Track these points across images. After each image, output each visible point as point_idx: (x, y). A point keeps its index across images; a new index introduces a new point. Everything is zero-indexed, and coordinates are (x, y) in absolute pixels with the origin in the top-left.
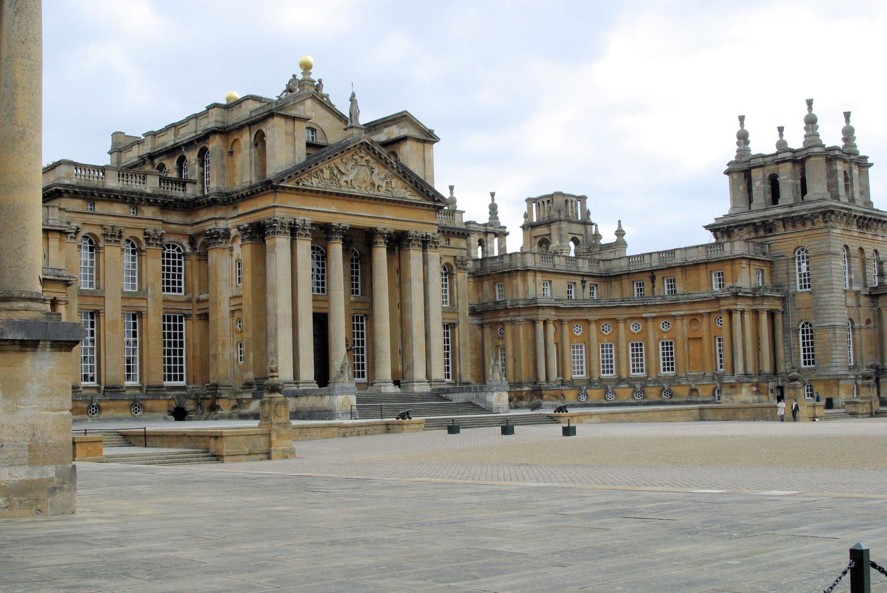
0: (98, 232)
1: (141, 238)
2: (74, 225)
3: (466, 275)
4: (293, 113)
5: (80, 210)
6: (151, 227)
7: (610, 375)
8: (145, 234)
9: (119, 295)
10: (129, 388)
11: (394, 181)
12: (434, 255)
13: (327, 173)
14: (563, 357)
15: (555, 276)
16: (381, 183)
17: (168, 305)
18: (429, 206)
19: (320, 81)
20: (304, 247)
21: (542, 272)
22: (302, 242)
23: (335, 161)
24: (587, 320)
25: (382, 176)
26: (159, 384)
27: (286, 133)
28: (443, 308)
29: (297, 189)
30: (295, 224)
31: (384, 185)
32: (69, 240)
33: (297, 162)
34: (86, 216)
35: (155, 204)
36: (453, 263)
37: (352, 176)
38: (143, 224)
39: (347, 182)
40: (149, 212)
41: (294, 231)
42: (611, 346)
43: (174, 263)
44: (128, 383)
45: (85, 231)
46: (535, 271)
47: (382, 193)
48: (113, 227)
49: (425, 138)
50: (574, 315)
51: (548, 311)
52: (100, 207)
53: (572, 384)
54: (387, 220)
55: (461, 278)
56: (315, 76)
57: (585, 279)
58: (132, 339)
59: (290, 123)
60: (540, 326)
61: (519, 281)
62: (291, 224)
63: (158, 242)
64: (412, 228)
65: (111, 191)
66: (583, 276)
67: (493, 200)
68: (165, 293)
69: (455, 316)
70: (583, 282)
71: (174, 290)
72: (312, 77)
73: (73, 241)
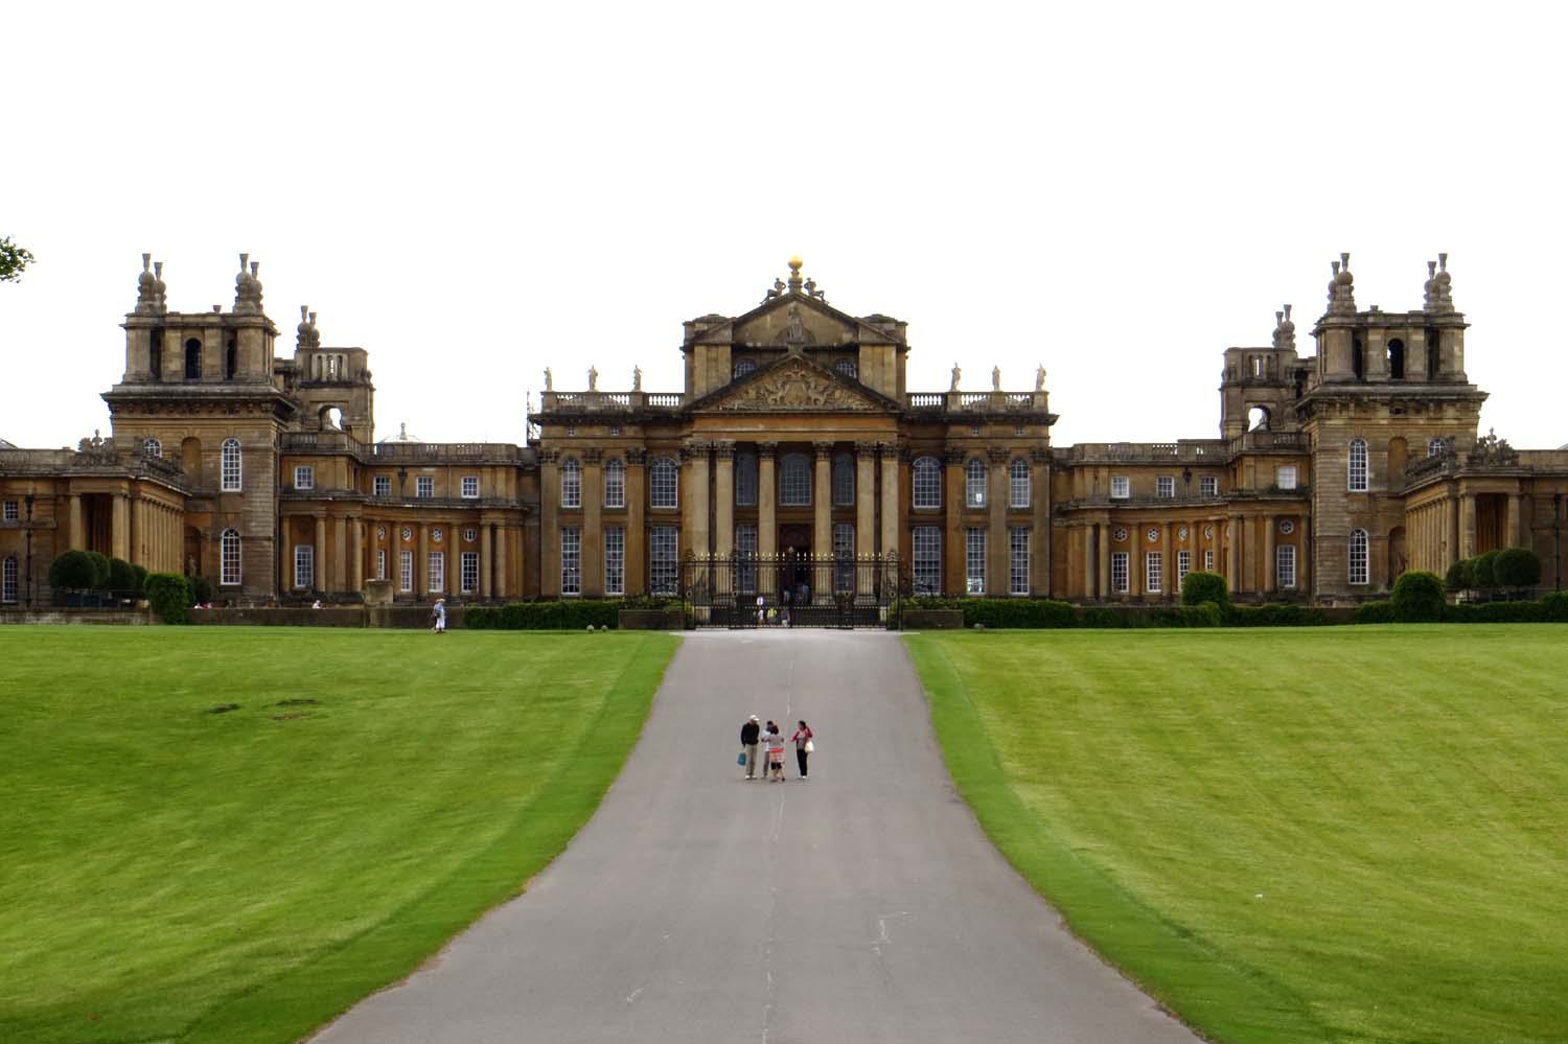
1: (623, 458)
2: (557, 449)
3: (1048, 468)
4: (711, 340)
5: (558, 434)
6: (632, 445)
8: (627, 452)
9: (599, 511)
11: (837, 394)
13: (752, 393)
16: (817, 396)
25: (821, 389)
31: (822, 399)
32: (550, 464)
34: (566, 441)
35: (633, 423)
38: (624, 443)
40: (630, 431)
41: (713, 455)
43: (667, 476)
44: (612, 594)
45: (567, 453)
46: (1096, 467)
47: (820, 405)
48: (593, 449)
49: (884, 340)
50: (1144, 518)
52: (576, 432)
54: (829, 432)
56: (804, 275)
57: (1190, 470)
59: (713, 349)
60: (1089, 531)
61: (1077, 477)
62: (708, 447)
63: (640, 460)
65: (594, 415)
69: (1029, 518)
70: (1188, 476)
72: (800, 276)
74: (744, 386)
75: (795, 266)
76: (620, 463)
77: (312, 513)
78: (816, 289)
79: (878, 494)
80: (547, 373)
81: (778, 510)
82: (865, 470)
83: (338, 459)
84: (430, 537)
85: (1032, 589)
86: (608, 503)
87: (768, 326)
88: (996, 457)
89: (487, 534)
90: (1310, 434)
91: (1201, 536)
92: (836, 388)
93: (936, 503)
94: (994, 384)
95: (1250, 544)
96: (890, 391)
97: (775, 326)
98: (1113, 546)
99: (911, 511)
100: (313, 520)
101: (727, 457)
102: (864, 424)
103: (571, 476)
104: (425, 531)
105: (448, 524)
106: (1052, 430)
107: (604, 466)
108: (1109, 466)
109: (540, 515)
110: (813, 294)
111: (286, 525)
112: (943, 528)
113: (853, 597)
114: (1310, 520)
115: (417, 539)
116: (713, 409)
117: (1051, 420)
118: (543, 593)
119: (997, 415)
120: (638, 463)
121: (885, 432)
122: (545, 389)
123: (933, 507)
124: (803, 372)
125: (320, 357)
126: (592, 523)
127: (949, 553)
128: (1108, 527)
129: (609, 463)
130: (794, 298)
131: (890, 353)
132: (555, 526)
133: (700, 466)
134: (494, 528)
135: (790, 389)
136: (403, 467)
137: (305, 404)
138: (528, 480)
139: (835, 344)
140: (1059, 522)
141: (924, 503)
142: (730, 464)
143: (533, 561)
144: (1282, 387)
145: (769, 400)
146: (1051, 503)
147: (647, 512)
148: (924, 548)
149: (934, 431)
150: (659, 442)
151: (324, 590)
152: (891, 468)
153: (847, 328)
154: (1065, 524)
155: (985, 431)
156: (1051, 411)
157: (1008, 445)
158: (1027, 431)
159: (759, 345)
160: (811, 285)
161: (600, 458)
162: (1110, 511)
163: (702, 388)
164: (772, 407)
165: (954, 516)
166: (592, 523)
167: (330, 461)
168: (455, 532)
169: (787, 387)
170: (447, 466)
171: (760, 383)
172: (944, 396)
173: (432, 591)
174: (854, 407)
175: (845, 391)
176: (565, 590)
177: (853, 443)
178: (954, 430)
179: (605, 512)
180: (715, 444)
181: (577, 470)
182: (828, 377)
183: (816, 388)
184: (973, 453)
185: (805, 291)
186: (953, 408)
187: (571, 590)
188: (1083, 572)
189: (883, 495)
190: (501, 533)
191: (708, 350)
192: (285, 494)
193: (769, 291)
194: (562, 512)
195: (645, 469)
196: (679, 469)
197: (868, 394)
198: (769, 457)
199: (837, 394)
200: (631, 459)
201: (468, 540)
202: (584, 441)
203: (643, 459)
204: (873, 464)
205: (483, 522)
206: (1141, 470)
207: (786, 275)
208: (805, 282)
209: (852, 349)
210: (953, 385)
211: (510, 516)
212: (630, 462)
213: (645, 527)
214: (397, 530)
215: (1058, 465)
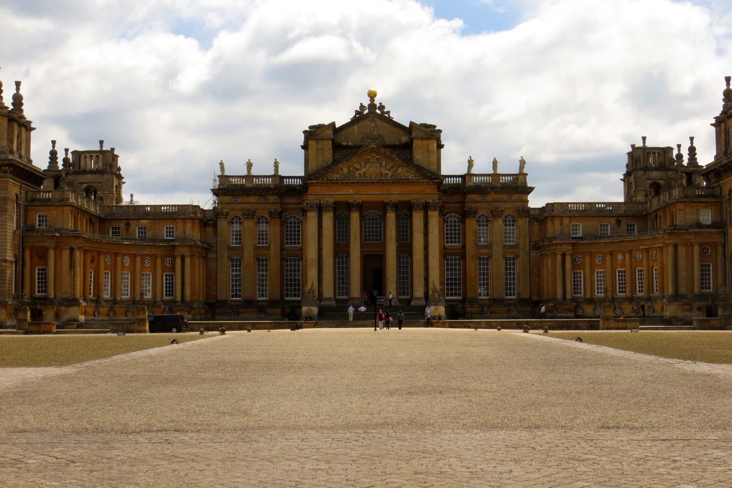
0: (240, 215)
1: (267, 216)
2: (225, 210)
5: (229, 201)
10: (258, 301)
13: (345, 170)
16: (387, 172)
18: (428, 182)
19: (381, 104)
25: (389, 166)
27: (317, 149)
29: (322, 183)
30: (320, 204)
31: (390, 173)
33: (325, 165)
34: (233, 205)
35: (273, 194)
39: (360, 174)
40: (272, 199)
41: (320, 209)
43: (295, 227)
44: (262, 299)
48: (249, 210)
51: (565, 247)
52: (240, 200)
53: (591, 301)
54: (396, 194)
56: (377, 102)
58: (264, 273)
59: (321, 142)
60: (559, 258)
61: (549, 224)
63: (278, 216)
66: (618, 217)
67: (692, 143)
70: (619, 222)
71: (295, 243)
73: (224, 220)
76: (266, 219)
77: (45, 244)
78: (385, 110)
79: (426, 235)
80: (222, 164)
81: (362, 245)
83: (65, 208)
85: (519, 294)
86: (259, 243)
88: (496, 214)
89: (178, 261)
90: (721, 188)
91: (633, 260)
92: (398, 166)
93: (459, 242)
94: (493, 169)
95: (682, 261)
96: (433, 168)
98: (574, 267)
99: (445, 248)
100: (46, 249)
101: (329, 210)
102: (416, 188)
103: (236, 227)
104: (138, 259)
105: (155, 255)
106: (530, 197)
107: (256, 221)
108: (570, 217)
110: (383, 113)
111: (27, 253)
112: (463, 257)
113: (410, 301)
114: (724, 245)
115: (133, 264)
119: (496, 187)
120: (277, 218)
121: (430, 194)
122: (220, 174)
123: (457, 244)
124: (377, 157)
125: (86, 156)
126: (248, 256)
127: (467, 272)
128: (572, 255)
129: (259, 219)
130: (371, 115)
131: (433, 145)
132: (225, 259)
133: (312, 216)
134: (183, 258)
135: (369, 168)
136: (128, 220)
137: (75, 184)
139: (397, 143)
140: (535, 254)
141: (451, 242)
142: (332, 215)
143: (211, 279)
144: (669, 170)
145: (356, 175)
146: (529, 242)
147: (282, 249)
148: (451, 270)
149: (457, 198)
150: (291, 206)
151: (52, 296)
152: (434, 218)
154: (539, 254)
155: (489, 198)
156: (529, 185)
157: (502, 206)
158: (515, 197)
159: (350, 144)
160: (382, 107)
161: (253, 215)
162: (573, 244)
163: (313, 166)
165: (470, 249)
166: (248, 256)
167: (60, 209)
168: (159, 260)
169: (368, 166)
170: (155, 219)
172: (463, 177)
173: (145, 297)
174: (410, 178)
176: (233, 296)
178: (470, 197)
179: (256, 248)
180: (322, 203)
181: (240, 223)
182: (393, 160)
183: (386, 166)
184: (481, 213)
185: (378, 111)
186: (469, 183)
187: (236, 297)
188: (555, 283)
189: (430, 235)
190: (188, 260)
191: (317, 143)
192: (26, 232)
193: (356, 111)
194: (230, 248)
195: (281, 222)
196: (302, 221)
197: (419, 169)
198: (356, 210)
199: (400, 170)
200: (273, 216)
201: (168, 265)
202: (245, 205)
203: (279, 215)
204: (422, 214)
207: (366, 102)
208: (378, 105)
209: (408, 147)
211: (195, 250)
212: (271, 218)
213: (281, 258)
214: (119, 259)
215: (533, 219)
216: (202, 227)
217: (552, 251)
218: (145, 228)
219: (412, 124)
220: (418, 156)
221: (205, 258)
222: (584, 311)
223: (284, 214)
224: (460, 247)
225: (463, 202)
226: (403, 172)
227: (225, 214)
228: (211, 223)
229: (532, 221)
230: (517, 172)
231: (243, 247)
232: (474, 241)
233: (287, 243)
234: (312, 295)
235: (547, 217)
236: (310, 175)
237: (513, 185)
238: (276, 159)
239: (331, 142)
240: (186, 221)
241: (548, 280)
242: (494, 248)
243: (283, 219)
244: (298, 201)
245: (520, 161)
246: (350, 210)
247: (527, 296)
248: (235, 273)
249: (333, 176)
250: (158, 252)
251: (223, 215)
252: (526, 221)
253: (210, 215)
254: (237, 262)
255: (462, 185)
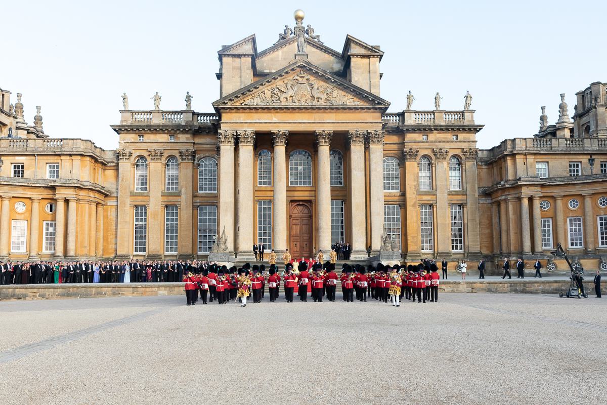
0: (145, 154)
1: (178, 156)
5: (133, 140)
6: (183, 148)
7: (578, 247)
11: (335, 94)
12: (377, 150)
14: (556, 230)
15: (554, 157)
17: (387, 198)
18: (368, 108)
20: (246, 151)
21: (535, 154)
22: (244, 147)
23: (277, 84)
24: (581, 195)
26: (418, 252)
27: (234, 68)
28: (450, 192)
31: (324, 97)
34: (137, 144)
36: (461, 154)
37: (291, 93)
38: (179, 146)
40: (183, 137)
42: (579, 220)
47: (322, 103)
49: (368, 53)
51: (533, 189)
55: (469, 165)
56: (305, 24)
57: (593, 157)
59: (237, 60)
60: (525, 202)
63: (190, 157)
64: (351, 128)
66: (591, 155)
68: (386, 191)
70: (591, 161)
71: (210, 189)
73: (127, 161)
74: (261, 87)
75: (298, 19)
82: (357, 151)
84: (12, 209)
87: (280, 59)
88: (439, 154)
89: (61, 206)
94: (436, 106)
96: (373, 91)
97: (284, 59)
108: (535, 154)
109: (117, 197)
116: (238, 104)
117: (476, 129)
118: (118, 254)
119: (441, 126)
122: (123, 109)
123: (395, 191)
124: (307, 78)
126: (155, 205)
134: (67, 201)
138: (110, 173)
140: (484, 201)
145: (282, 99)
146: (478, 188)
147: (194, 196)
149: (395, 139)
153: (337, 60)
154: (490, 201)
155: (433, 137)
156: (476, 123)
157: (447, 147)
158: (461, 136)
162: (542, 186)
164: (283, 104)
168: (36, 205)
169: (295, 88)
170: (34, 155)
171: (274, 86)
172: (402, 115)
174: (348, 104)
175: (340, 92)
177: (348, 131)
178: (409, 137)
179: (163, 195)
180: (238, 132)
183: (318, 89)
186: (411, 120)
190: (72, 205)
193: (280, 35)
194: (133, 194)
197: (359, 93)
199: (335, 94)
200: (184, 157)
202: (148, 144)
204: (363, 147)
205: (57, 197)
206: (557, 157)
207: (292, 25)
210: (409, 104)
211: (83, 193)
212: (183, 159)
213: (194, 206)
216: (100, 171)
217: (514, 196)
218: (23, 167)
219: (349, 42)
220: (358, 78)
221: (98, 204)
222: (556, 267)
223: (197, 156)
224: (398, 195)
225: (403, 143)
226: (341, 97)
227: (128, 154)
228: (112, 164)
229: (480, 163)
230: (462, 109)
231: (148, 193)
232: (415, 186)
233: (201, 189)
234: (223, 247)
235: (507, 155)
236: (226, 98)
237: (459, 124)
238: (188, 93)
239: (249, 60)
240: (74, 157)
241: (508, 230)
242: (438, 195)
243: (196, 162)
244: (213, 141)
245: (467, 97)
246: (273, 144)
247: (477, 250)
248: (139, 223)
249: (252, 100)
250: (35, 194)
251: (126, 156)
252: (474, 164)
253: (109, 157)
254: (141, 209)
255: (400, 124)
